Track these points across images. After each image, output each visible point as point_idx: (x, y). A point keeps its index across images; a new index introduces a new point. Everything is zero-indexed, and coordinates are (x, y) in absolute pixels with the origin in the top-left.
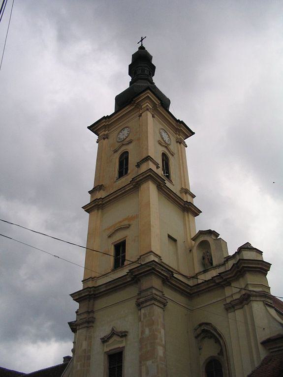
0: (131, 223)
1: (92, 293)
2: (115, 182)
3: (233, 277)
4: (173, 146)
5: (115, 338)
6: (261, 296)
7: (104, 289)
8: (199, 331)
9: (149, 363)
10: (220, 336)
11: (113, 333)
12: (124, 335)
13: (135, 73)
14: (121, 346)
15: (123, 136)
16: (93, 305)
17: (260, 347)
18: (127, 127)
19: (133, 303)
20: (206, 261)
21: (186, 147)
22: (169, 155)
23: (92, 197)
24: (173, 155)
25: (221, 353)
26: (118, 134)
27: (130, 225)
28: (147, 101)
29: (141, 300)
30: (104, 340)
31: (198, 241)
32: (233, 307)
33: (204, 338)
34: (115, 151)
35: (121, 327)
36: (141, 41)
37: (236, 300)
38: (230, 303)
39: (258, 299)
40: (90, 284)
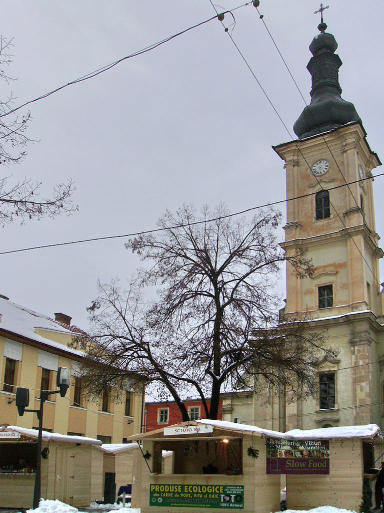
0: (338, 271)
9: (363, 384)
23: (287, 233)
27: (337, 272)
28: (354, 136)
36: (321, 10)
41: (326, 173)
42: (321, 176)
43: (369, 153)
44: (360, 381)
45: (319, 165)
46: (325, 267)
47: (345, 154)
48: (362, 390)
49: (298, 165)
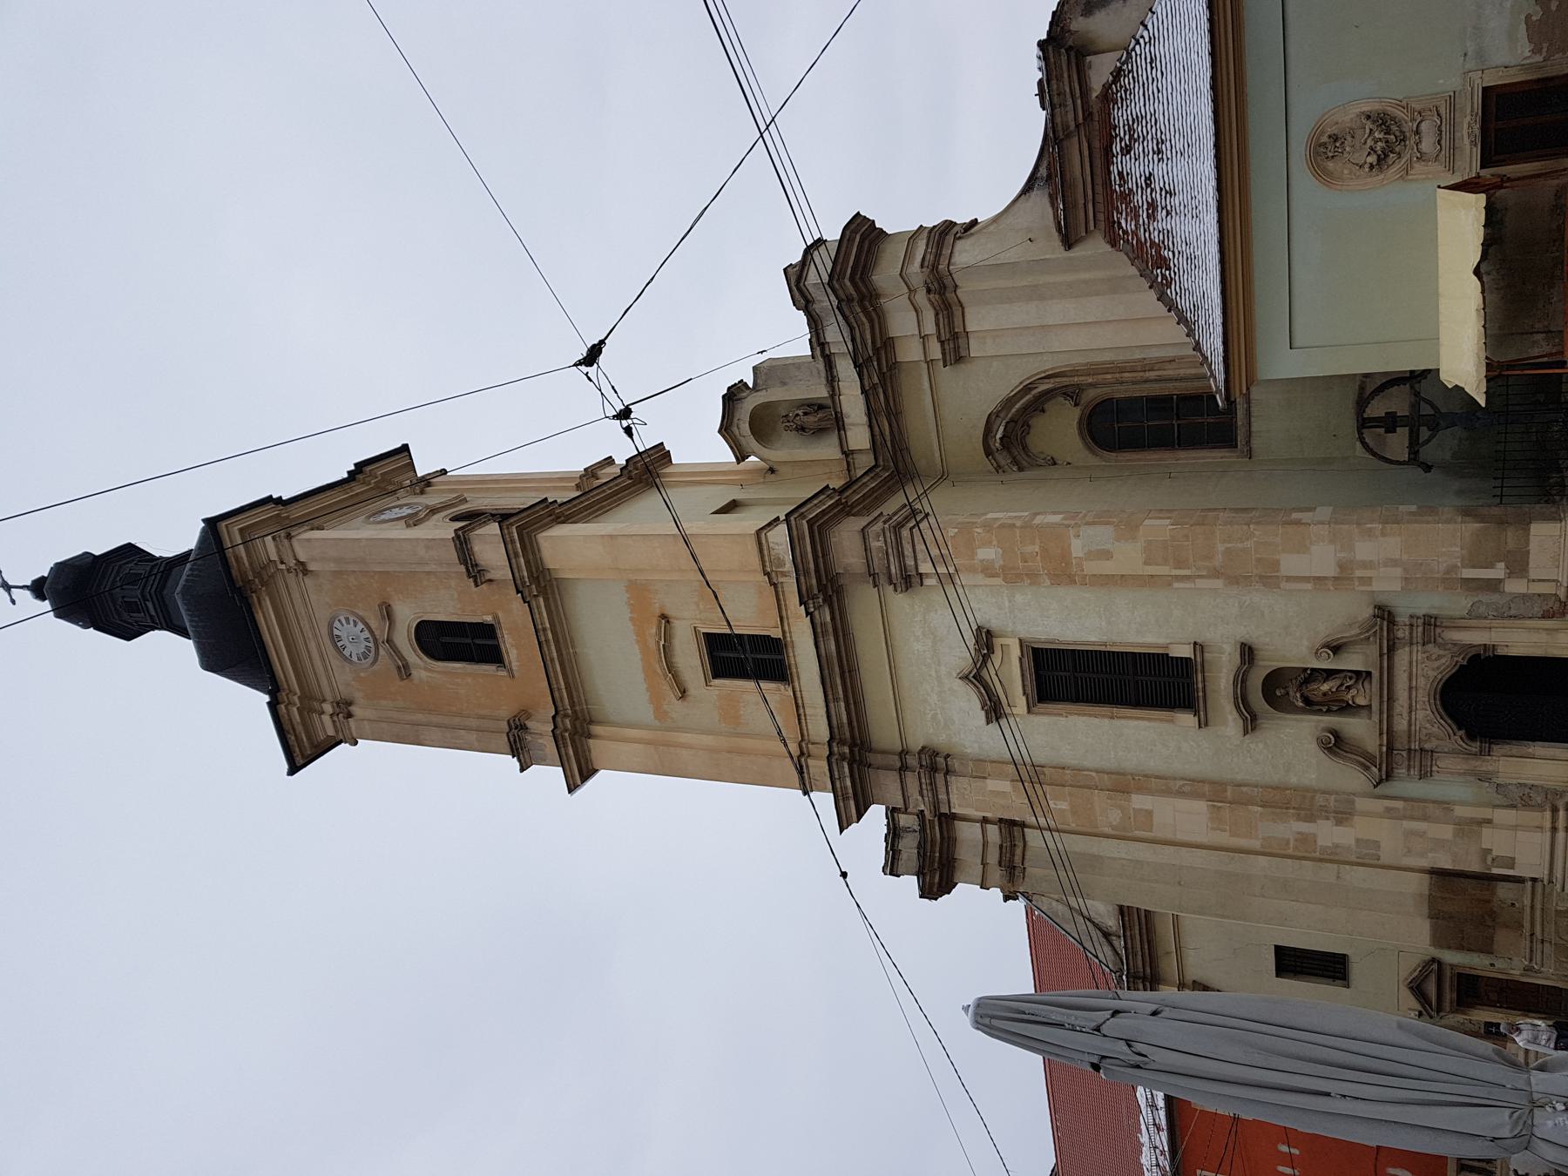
0: (658, 613)
1: (846, 750)
2: (512, 675)
3: (871, 321)
4: (432, 499)
5: (989, 674)
6: (940, 245)
7: (842, 704)
8: (1003, 459)
9: (1077, 548)
10: (1027, 389)
11: (976, 677)
12: (985, 641)
13: (133, 607)
14: (1016, 652)
15: (353, 636)
16: (884, 752)
17: (1078, 252)
18: (331, 627)
19: (899, 602)
20: (811, 420)
21: (444, 472)
22: (463, 508)
23: (542, 761)
24: (465, 501)
25: (1072, 393)
26: (348, 660)
27: (663, 616)
29: (893, 570)
30: (994, 710)
31: (750, 442)
32: (955, 336)
33: (1025, 448)
34: (404, 670)
35: (960, 655)
37: (937, 325)
38: (942, 343)
39: (946, 252)
40: (819, 767)
41: (366, 624)
42: (375, 640)
43: (353, 484)
44: (1065, 555)
45: (345, 642)
46: (644, 650)
47: (312, 567)
48: (1107, 555)
49: (349, 703)
